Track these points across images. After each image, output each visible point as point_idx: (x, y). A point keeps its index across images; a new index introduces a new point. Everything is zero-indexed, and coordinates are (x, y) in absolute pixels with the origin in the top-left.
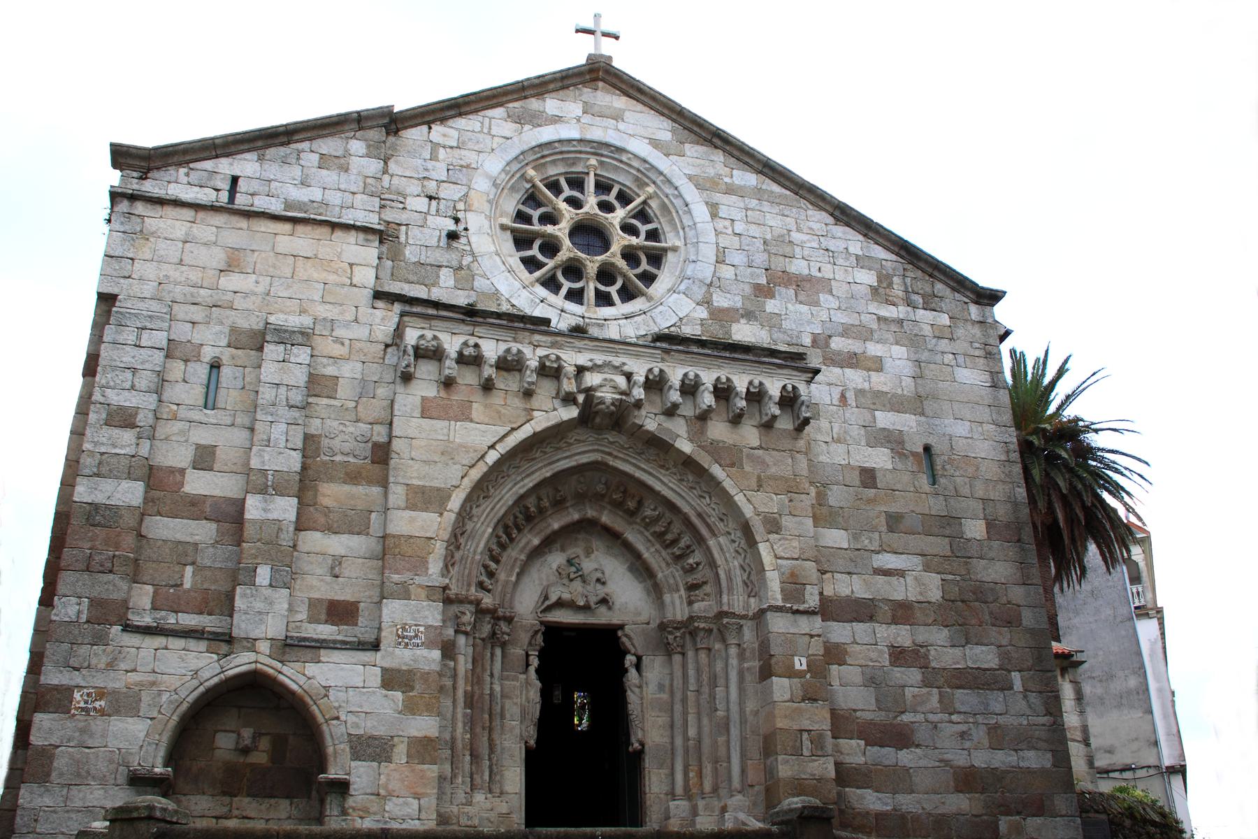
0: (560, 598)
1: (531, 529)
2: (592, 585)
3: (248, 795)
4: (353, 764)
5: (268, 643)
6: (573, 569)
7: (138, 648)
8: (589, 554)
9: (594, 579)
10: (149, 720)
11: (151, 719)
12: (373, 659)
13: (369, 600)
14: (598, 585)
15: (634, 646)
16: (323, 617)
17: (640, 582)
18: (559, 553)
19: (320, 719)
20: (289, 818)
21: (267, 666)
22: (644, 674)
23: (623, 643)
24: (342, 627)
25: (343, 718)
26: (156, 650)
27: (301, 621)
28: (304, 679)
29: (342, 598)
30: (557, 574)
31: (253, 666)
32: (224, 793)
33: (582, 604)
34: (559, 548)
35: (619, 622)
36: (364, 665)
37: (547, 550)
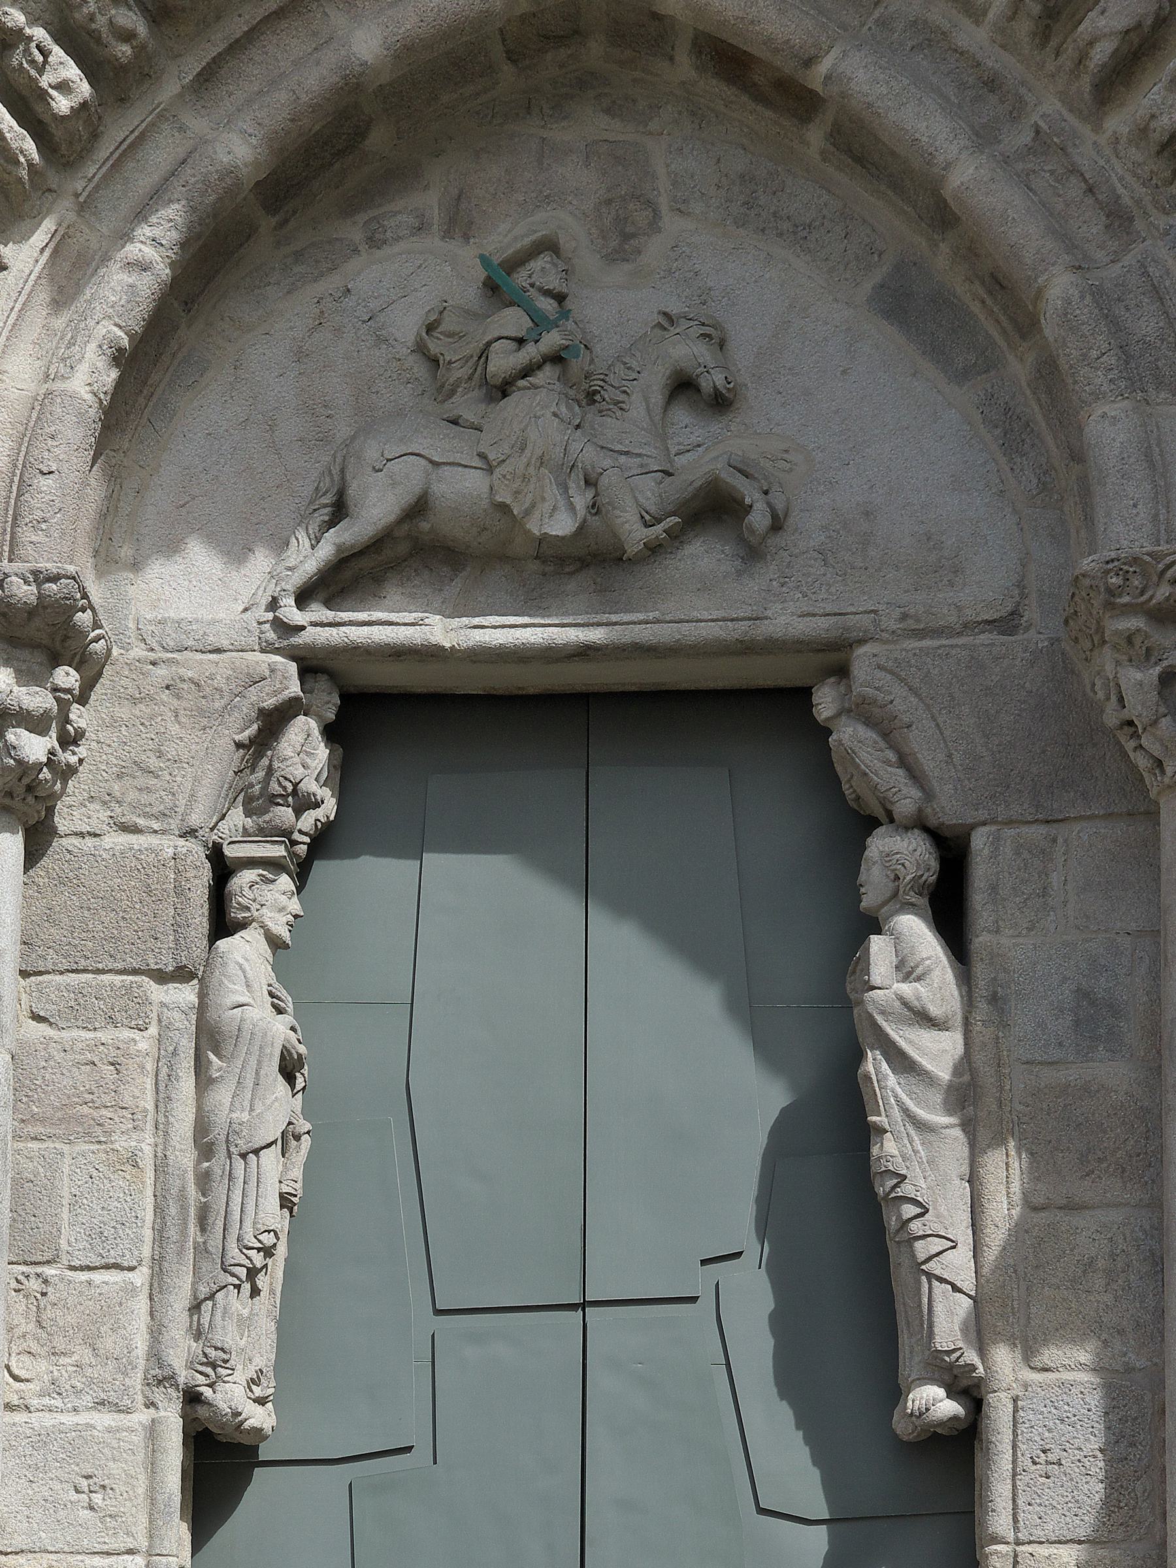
0: (419, 508)
1: (207, 77)
2: (637, 410)
6: (513, 321)
8: (626, 237)
9: (655, 380)
14: (681, 415)
15: (915, 775)
17: (962, 376)
18: (434, 242)
22: (981, 940)
23: (849, 756)
30: (420, 369)
33: (561, 526)
34: (436, 216)
35: (817, 627)
37: (354, 232)
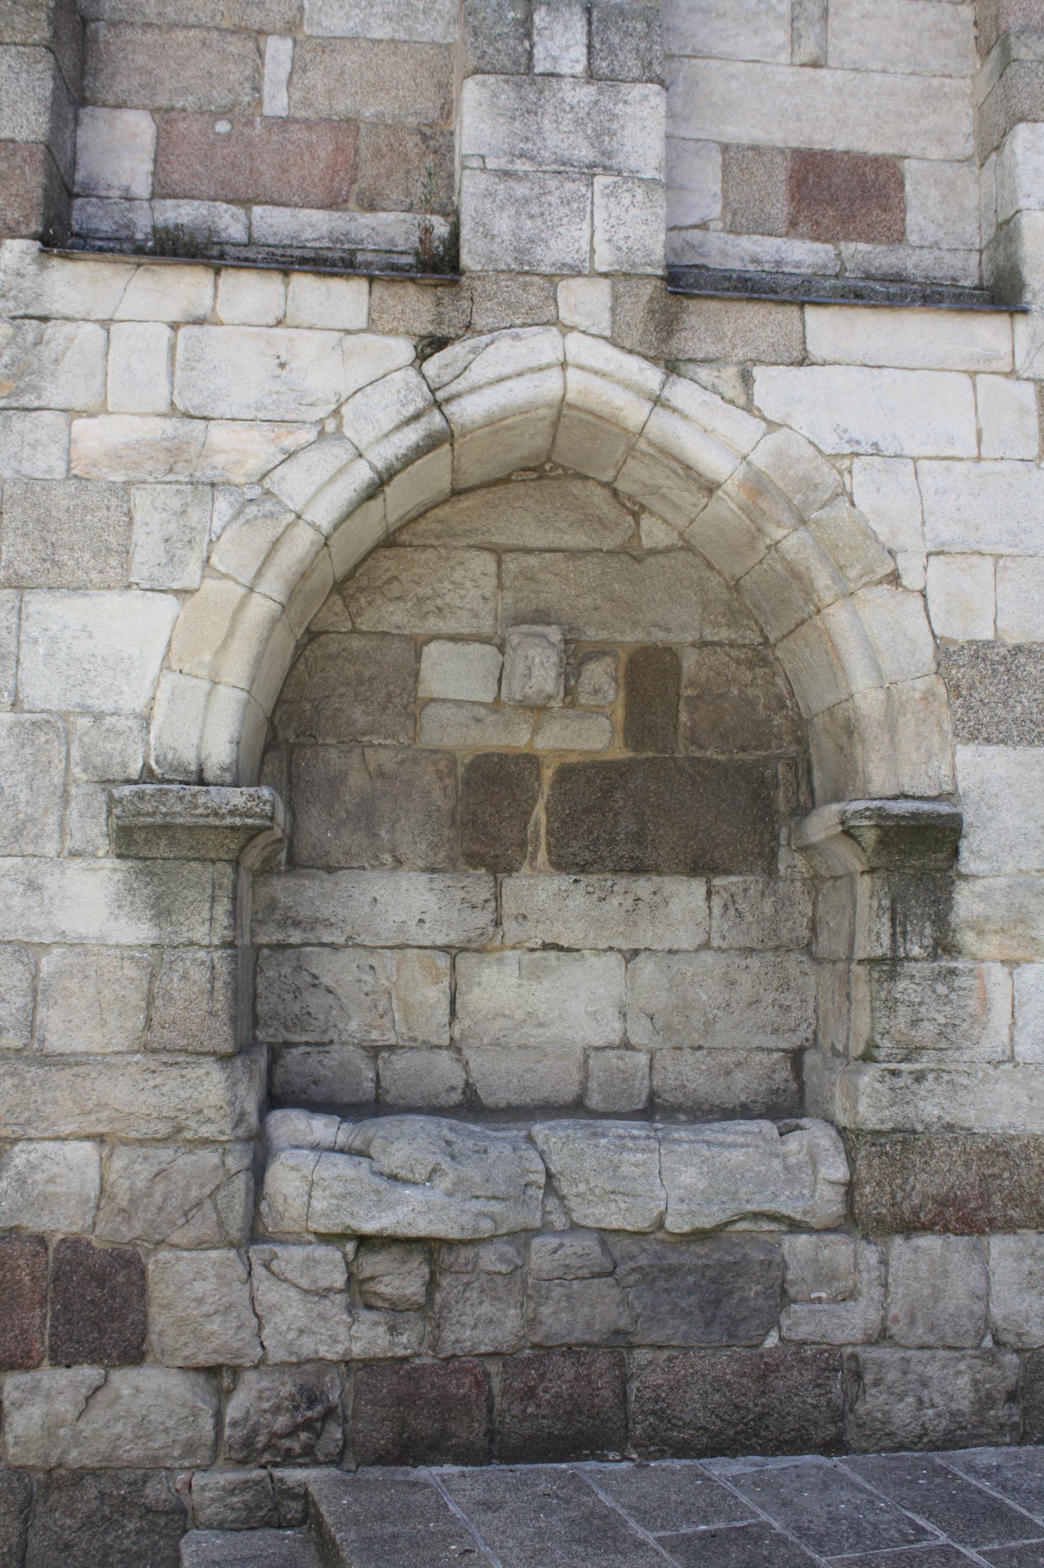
3: (559, 865)
4: (965, 753)
5: (598, 294)
7: (106, 324)
10: (169, 601)
11: (183, 593)
12: (1005, 347)
13: (935, 153)
16: (779, 209)
19: (822, 579)
20: (706, 946)
21: (604, 375)
24: (848, 248)
25: (912, 579)
26: (175, 326)
27: (703, 226)
28: (754, 427)
29: (841, 145)
31: (550, 386)
32: (474, 860)
36: (973, 374)
